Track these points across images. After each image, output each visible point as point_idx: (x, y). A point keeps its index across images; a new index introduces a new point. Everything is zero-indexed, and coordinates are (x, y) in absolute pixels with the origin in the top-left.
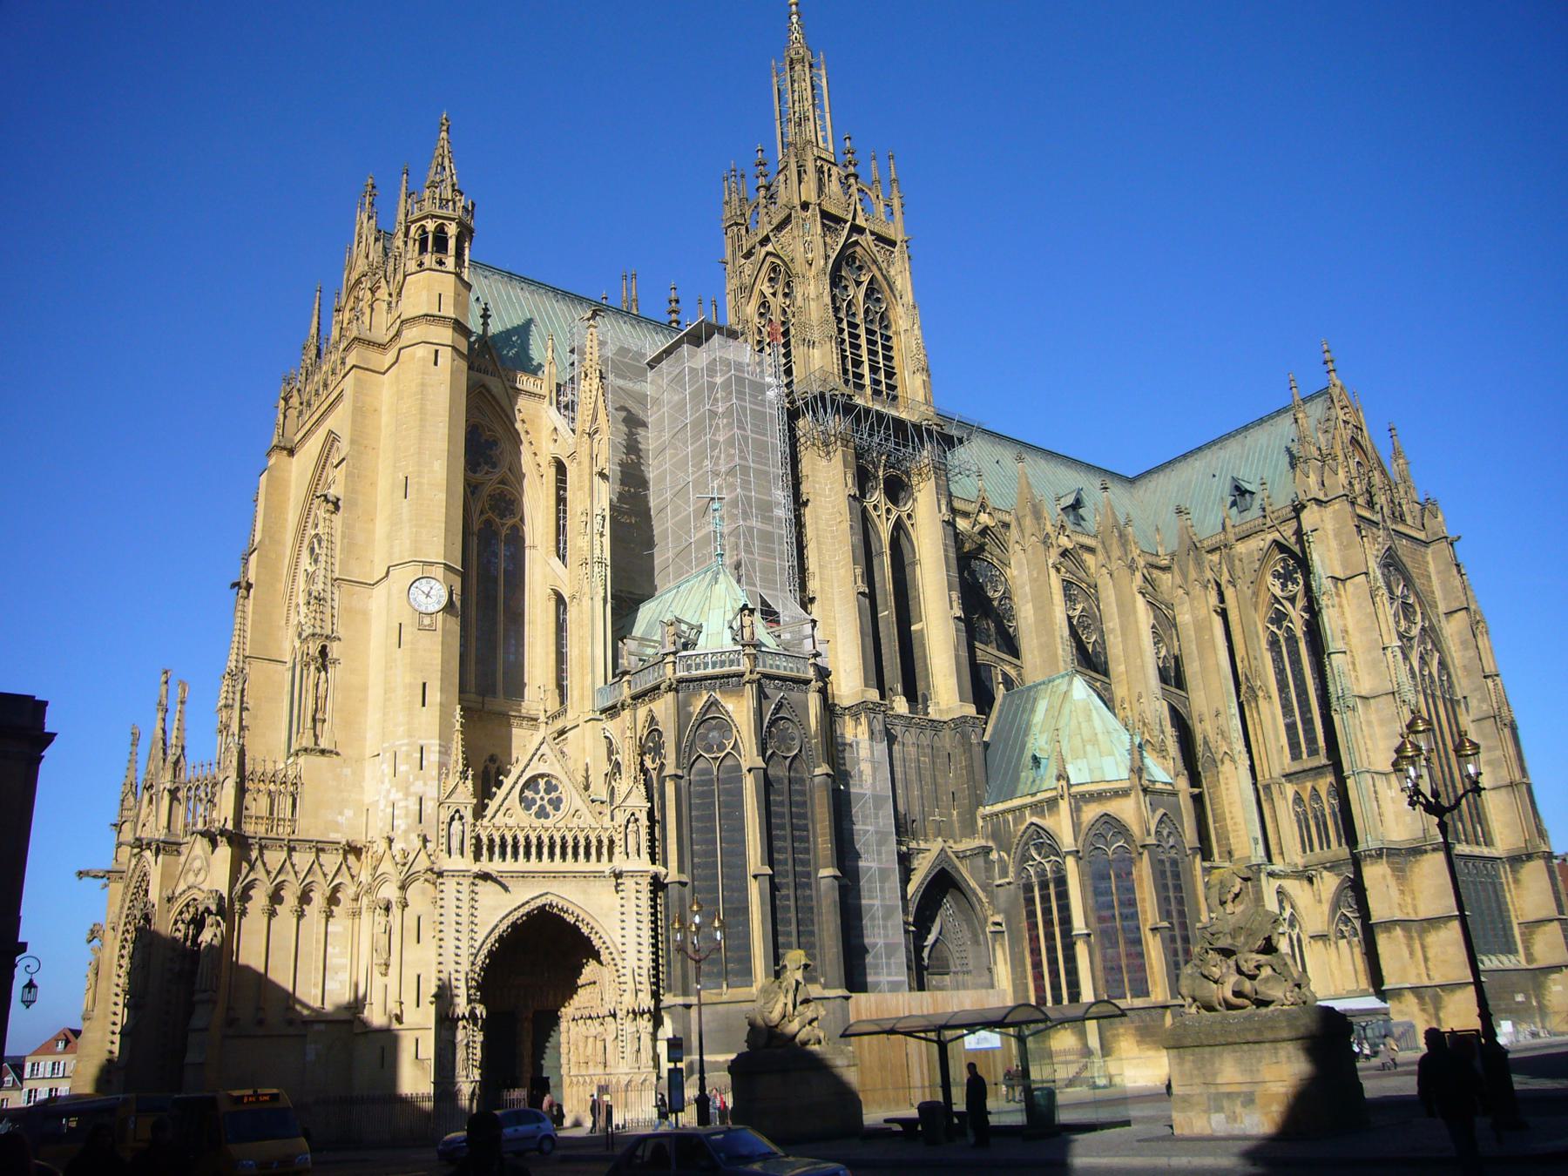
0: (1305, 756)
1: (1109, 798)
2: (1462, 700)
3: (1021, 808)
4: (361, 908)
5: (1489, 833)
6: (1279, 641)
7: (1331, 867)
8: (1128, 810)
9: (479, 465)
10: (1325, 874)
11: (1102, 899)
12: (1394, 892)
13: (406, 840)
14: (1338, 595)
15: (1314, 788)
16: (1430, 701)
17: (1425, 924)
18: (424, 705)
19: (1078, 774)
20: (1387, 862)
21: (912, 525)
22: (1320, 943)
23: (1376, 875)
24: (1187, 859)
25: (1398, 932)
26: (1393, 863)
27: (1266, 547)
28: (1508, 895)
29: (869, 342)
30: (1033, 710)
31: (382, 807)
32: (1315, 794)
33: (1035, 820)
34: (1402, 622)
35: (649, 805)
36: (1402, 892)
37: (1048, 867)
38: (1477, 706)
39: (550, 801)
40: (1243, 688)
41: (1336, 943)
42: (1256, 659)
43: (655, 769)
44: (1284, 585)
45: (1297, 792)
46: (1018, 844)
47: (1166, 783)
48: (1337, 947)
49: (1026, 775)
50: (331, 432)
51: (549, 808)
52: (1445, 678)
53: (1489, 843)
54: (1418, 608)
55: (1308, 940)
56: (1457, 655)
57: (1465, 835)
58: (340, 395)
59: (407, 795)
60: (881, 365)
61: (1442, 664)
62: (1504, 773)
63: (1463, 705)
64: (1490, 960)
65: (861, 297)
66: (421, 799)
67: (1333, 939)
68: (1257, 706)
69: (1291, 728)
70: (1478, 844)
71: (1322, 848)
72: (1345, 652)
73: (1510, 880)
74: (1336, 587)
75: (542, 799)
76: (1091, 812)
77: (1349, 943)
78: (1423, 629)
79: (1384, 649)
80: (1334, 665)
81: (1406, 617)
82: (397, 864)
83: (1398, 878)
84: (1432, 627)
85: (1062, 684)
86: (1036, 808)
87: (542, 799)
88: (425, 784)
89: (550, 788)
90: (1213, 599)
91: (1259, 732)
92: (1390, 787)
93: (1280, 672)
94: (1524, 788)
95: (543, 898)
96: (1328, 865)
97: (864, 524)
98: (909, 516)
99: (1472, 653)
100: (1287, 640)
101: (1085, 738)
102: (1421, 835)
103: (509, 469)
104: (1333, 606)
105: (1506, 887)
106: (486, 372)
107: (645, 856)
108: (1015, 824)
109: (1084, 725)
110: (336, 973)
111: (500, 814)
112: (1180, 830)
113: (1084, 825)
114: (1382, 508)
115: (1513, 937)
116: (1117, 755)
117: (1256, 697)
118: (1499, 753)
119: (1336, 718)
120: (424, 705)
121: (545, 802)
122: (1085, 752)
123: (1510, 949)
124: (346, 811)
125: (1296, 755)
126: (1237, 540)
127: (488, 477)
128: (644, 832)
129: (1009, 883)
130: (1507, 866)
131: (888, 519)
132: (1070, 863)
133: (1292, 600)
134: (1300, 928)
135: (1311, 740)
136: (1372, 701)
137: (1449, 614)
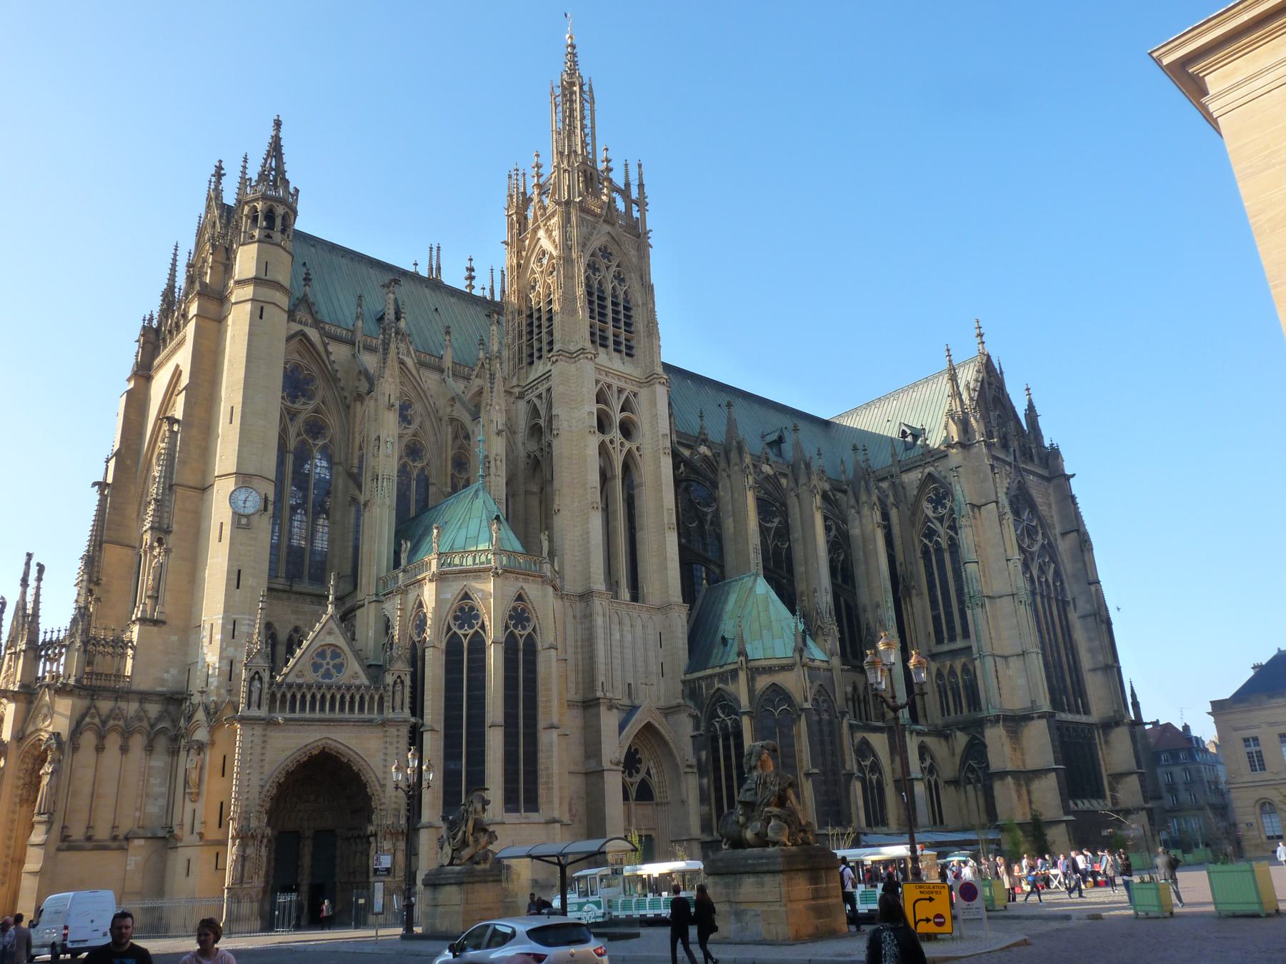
0: (946, 641)
2: (1071, 602)
3: (711, 676)
4: (179, 748)
5: (1088, 704)
8: (793, 682)
9: (297, 397)
10: (959, 734)
12: (1007, 749)
13: (219, 695)
14: (975, 518)
15: (951, 666)
16: (1046, 601)
17: (1031, 775)
18: (238, 588)
19: (756, 651)
20: (1003, 726)
21: (640, 455)
22: (952, 788)
23: (995, 737)
24: (836, 720)
25: (1010, 780)
26: (1008, 727)
27: (924, 478)
28: (1100, 754)
29: (615, 312)
30: (725, 602)
31: (199, 667)
32: (952, 672)
33: (721, 685)
34: (1026, 539)
35: (412, 669)
36: (1014, 749)
37: (729, 723)
38: (1083, 606)
39: (334, 666)
40: (901, 587)
41: (965, 788)
42: (911, 563)
43: (419, 641)
44: (935, 509)
45: (938, 669)
46: (708, 705)
47: (823, 661)
48: (966, 792)
49: (717, 651)
50: (177, 366)
51: (333, 671)
52: (1058, 584)
53: (1087, 712)
54: (1039, 529)
55: (943, 784)
56: (1068, 566)
57: (1068, 705)
58: (184, 339)
59: (221, 658)
60: (623, 330)
61: (1057, 574)
62: (1100, 658)
63: (1072, 605)
64: (1076, 805)
65: (610, 276)
66: (232, 662)
67: (963, 784)
68: (911, 602)
69: (936, 619)
70: (1078, 712)
71: (956, 713)
72: (977, 562)
73: (1102, 741)
74: (973, 511)
75: (328, 664)
76: (763, 682)
77: (975, 787)
78: (1043, 545)
79: (1007, 560)
80: (968, 571)
81: (1029, 536)
82: (209, 713)
83: (1011, 738)
84: (1050, 544)
85: (748, 581)
86: (723, 677)
87: (328, 664)
88: (236, 650)
89: (335, 655)
90: (877, 516)
91: (911, 621)
92: (1008, 667)
93: (930, 574)
94: (1116, 669)
95: (324, 741)
97: (603, 450)
98: (638, 449)
99: (1080, 565)
100: (936, 550)
102: (1030, 705)
103: (323, 402)
104: (971, 526)
105: (1099, 747)
106: (306, 324)
107: (407, 711)
108: (707, 689)
109: (762, 615)
110: (156, 799)
111: (292, 675)
112: (832, 697)
113: (757, 693)
114: (1014, 451)
115: (1103, 785)
116: (785, 637)
117: (910, 596)
118: (1097, 643)
119: (969, 612)
120: (238, 588)
121: (330, 666)
122: (761, 636)
123: (1099, 794)
124: (171, 670)
125: (940, 641)
126: (901, 472)
127: (305, 407)
128: (407, 691)
130: (1101, 732)
131: (621, 451)
132: (746, 723)
133: (941, 520)
134: (937, 775)
135: (951, 628)
136: (997, 600)
137: (1064, 534)
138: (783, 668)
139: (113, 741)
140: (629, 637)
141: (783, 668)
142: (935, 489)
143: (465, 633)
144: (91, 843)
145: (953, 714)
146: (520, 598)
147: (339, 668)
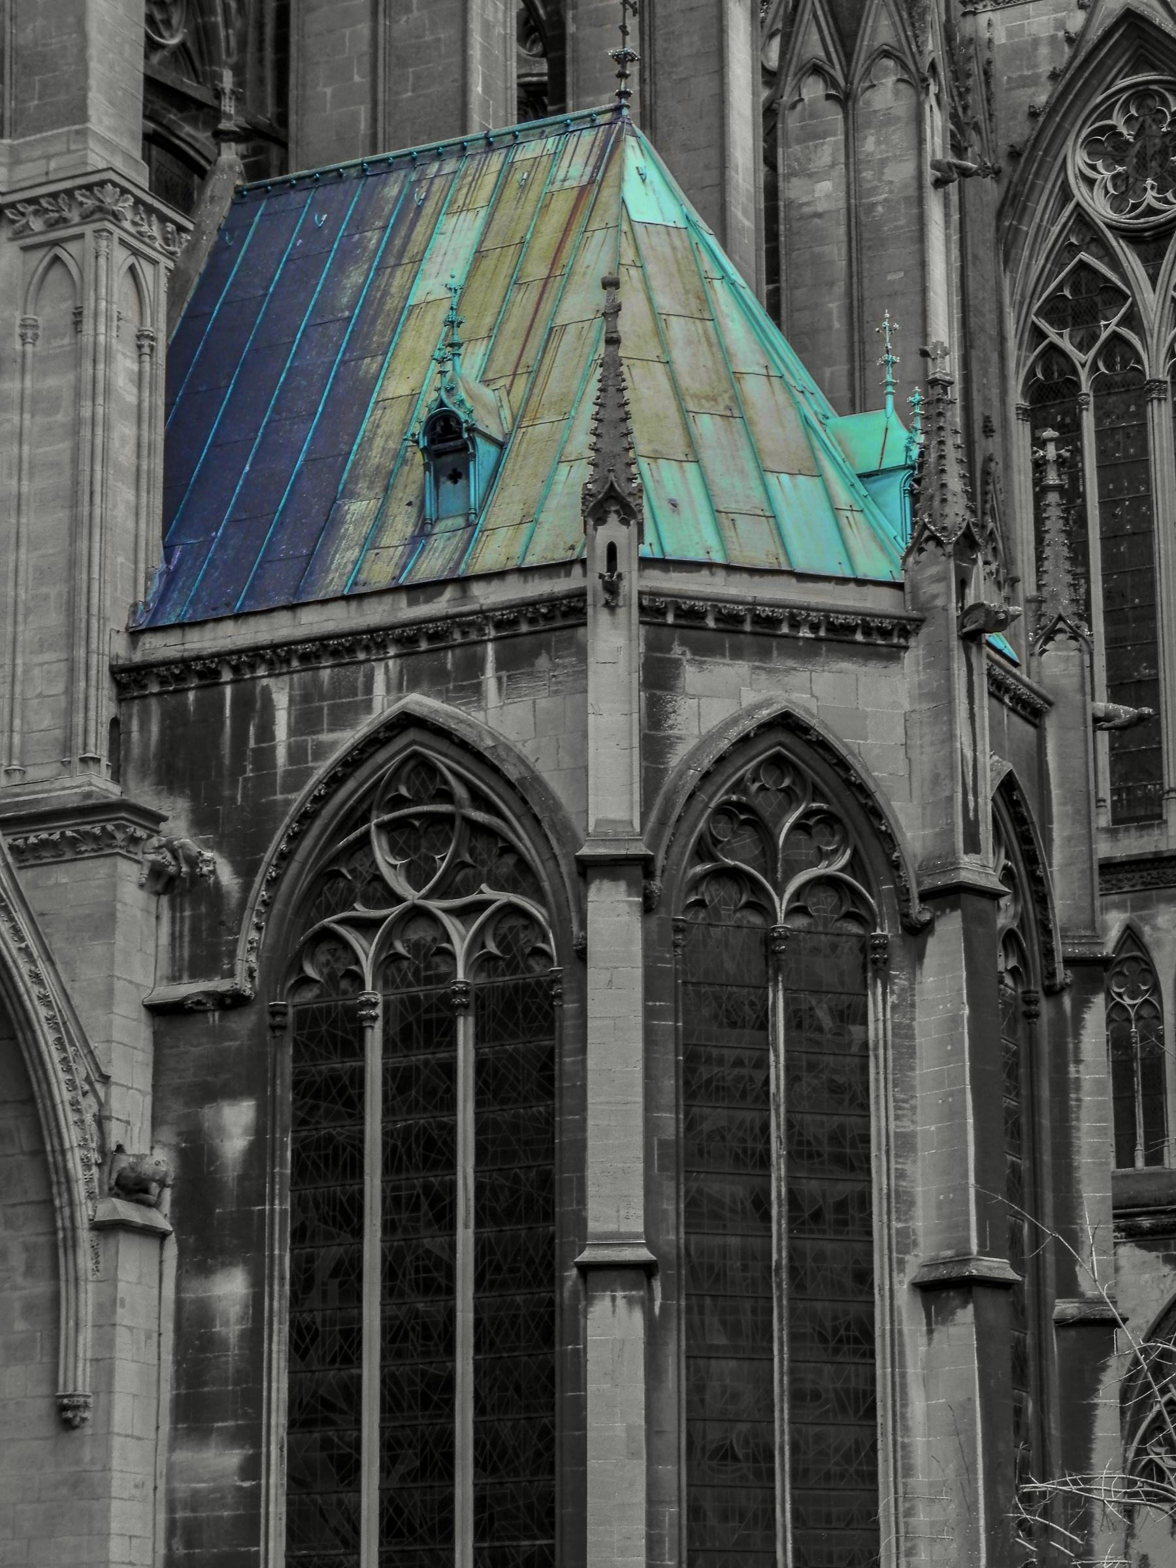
1: (809, 651)
6: (1077, 385)
7: (1153, 1231)
11: (715, 1116)
27: (1094, 35)
37: (460, 937)
46: (306, 818)
96: (1146, 1223)
100: (1102, 386)
101: (685, 381)
108: (305, 722)
109: (678, 329)
122: (691, 442)
129: (232, 1002)
142: (1141, 94)
145: (1140, 1163)
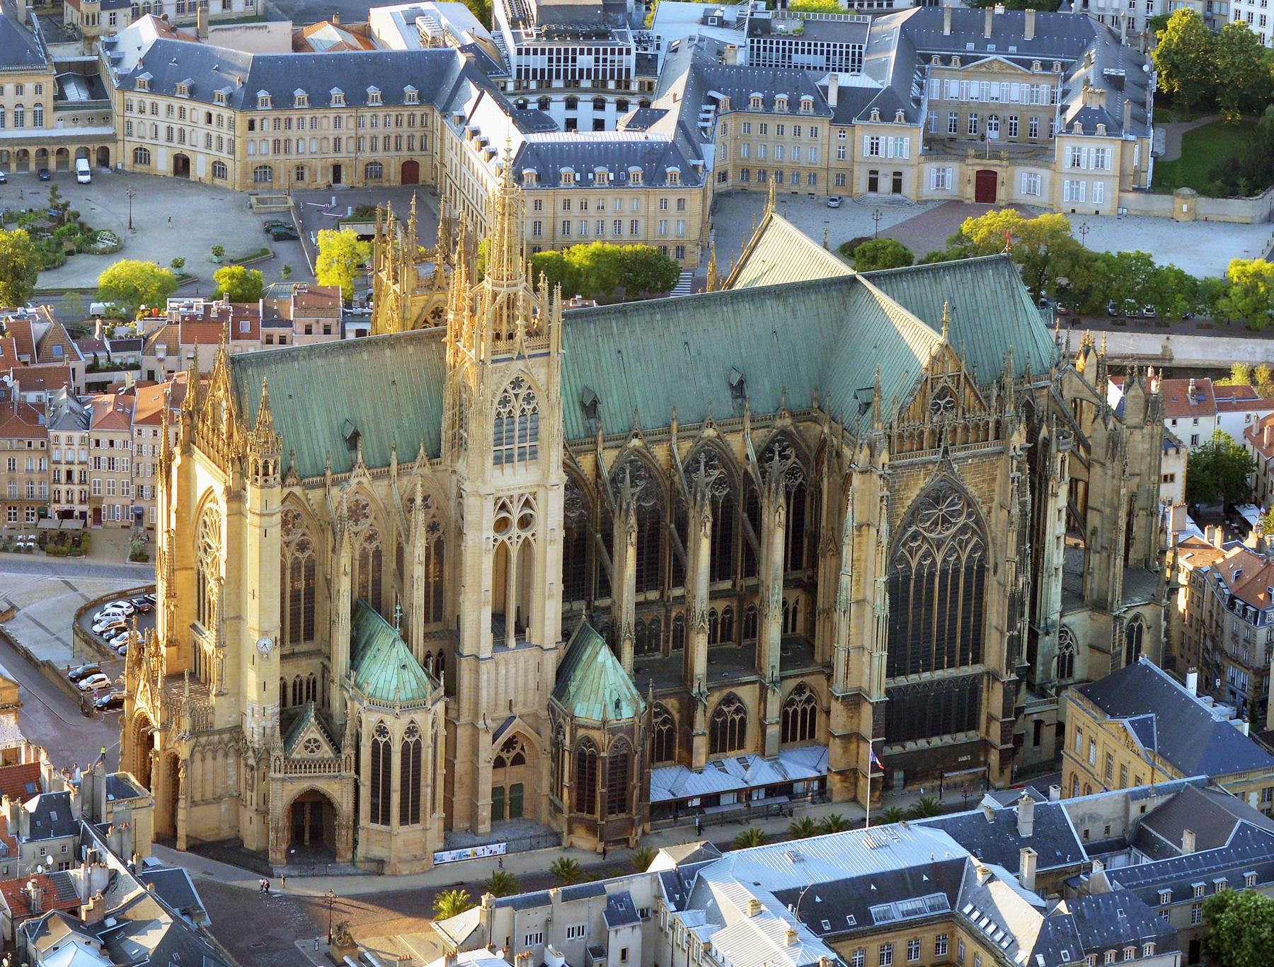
138: (594, 728)
139: (209, 757)
140: (512, 671)
141: (594, 728)
143: (382, 740)
144: (205, 802)
146: (412, 722)
147: (318, 748)
